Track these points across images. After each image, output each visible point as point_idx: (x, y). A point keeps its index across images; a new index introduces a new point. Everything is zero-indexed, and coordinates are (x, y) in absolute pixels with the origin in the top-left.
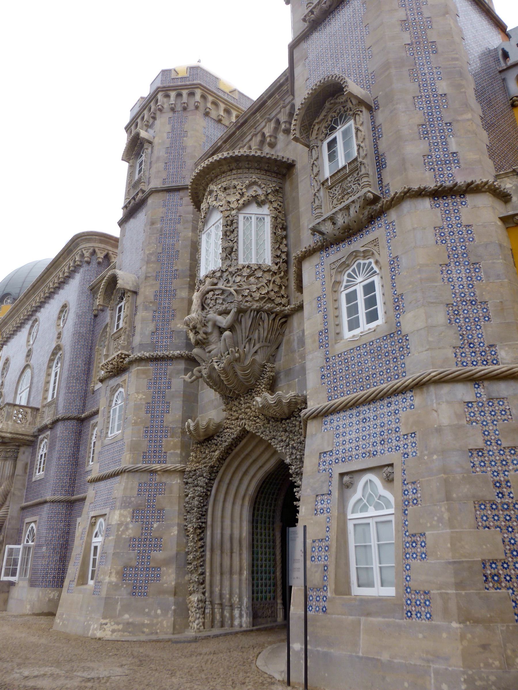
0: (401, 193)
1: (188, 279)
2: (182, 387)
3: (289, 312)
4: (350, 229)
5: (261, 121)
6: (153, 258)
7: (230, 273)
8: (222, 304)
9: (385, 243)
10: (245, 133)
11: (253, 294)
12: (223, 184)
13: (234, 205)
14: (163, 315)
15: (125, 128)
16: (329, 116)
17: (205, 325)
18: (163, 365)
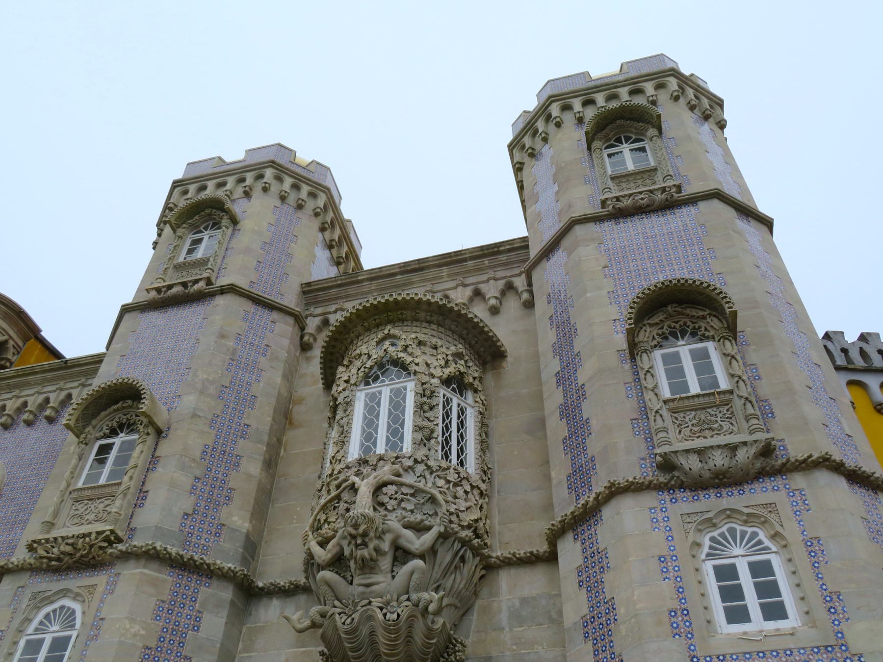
0: (819, 458)
2: (220, 635)
3: (498, 562)
4: (725, 477)
5: (445, 279)
6: (212, 390)
8: (412, 511)
9: (791, 514)
10: (411, 283)
12: (418, 335)
13: (437, 372)
14: (211, 490)
15: (174, 182)
16: (666, 324)
17: (379, 538)
18: (192, 581)
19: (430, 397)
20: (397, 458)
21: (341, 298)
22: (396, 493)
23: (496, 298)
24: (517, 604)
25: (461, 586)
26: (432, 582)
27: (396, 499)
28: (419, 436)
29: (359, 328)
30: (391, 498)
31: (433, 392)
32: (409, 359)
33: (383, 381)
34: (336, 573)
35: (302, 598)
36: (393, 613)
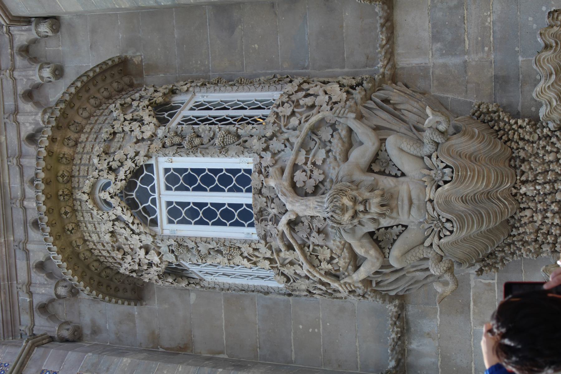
1: (220, 370)
3: (389, 66)
7: (274, 135)
11: (333, 100)
13: (148, 131)
19: (183, 137)
20: (260, 172)
21: (11, 286)
22: (304, 171)
23: (41, 68)
24: (439, 45)
25: (415, 104)
26: (411, 134)
27: (312, 171)
28: (233, 149)
29: (74, 237)
30: (310, 178)
31: (176, 134)
32: (129, 164)
33: (154, 201)
34: (392, 244)
35: (411, 310)
36: (444, 174)
